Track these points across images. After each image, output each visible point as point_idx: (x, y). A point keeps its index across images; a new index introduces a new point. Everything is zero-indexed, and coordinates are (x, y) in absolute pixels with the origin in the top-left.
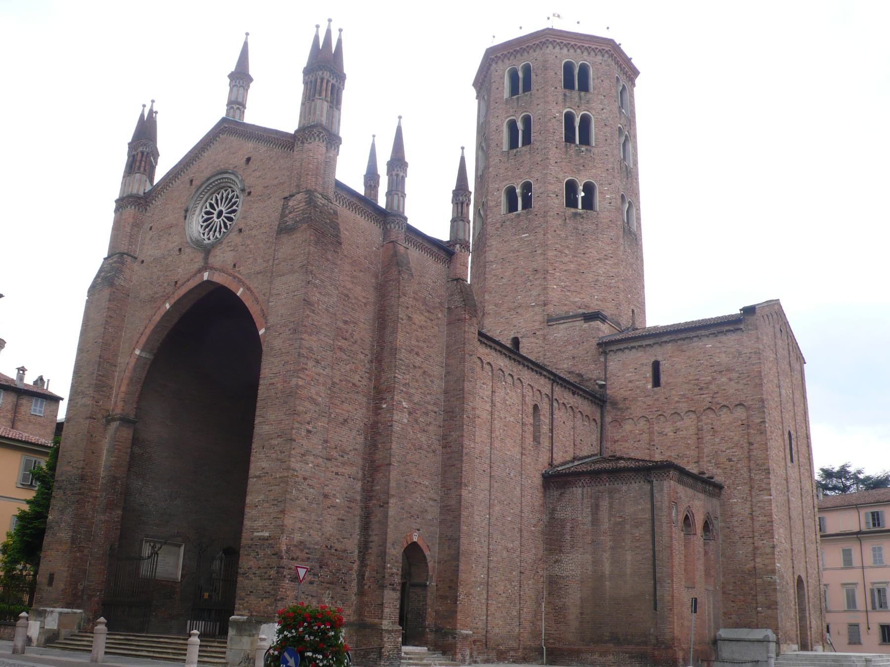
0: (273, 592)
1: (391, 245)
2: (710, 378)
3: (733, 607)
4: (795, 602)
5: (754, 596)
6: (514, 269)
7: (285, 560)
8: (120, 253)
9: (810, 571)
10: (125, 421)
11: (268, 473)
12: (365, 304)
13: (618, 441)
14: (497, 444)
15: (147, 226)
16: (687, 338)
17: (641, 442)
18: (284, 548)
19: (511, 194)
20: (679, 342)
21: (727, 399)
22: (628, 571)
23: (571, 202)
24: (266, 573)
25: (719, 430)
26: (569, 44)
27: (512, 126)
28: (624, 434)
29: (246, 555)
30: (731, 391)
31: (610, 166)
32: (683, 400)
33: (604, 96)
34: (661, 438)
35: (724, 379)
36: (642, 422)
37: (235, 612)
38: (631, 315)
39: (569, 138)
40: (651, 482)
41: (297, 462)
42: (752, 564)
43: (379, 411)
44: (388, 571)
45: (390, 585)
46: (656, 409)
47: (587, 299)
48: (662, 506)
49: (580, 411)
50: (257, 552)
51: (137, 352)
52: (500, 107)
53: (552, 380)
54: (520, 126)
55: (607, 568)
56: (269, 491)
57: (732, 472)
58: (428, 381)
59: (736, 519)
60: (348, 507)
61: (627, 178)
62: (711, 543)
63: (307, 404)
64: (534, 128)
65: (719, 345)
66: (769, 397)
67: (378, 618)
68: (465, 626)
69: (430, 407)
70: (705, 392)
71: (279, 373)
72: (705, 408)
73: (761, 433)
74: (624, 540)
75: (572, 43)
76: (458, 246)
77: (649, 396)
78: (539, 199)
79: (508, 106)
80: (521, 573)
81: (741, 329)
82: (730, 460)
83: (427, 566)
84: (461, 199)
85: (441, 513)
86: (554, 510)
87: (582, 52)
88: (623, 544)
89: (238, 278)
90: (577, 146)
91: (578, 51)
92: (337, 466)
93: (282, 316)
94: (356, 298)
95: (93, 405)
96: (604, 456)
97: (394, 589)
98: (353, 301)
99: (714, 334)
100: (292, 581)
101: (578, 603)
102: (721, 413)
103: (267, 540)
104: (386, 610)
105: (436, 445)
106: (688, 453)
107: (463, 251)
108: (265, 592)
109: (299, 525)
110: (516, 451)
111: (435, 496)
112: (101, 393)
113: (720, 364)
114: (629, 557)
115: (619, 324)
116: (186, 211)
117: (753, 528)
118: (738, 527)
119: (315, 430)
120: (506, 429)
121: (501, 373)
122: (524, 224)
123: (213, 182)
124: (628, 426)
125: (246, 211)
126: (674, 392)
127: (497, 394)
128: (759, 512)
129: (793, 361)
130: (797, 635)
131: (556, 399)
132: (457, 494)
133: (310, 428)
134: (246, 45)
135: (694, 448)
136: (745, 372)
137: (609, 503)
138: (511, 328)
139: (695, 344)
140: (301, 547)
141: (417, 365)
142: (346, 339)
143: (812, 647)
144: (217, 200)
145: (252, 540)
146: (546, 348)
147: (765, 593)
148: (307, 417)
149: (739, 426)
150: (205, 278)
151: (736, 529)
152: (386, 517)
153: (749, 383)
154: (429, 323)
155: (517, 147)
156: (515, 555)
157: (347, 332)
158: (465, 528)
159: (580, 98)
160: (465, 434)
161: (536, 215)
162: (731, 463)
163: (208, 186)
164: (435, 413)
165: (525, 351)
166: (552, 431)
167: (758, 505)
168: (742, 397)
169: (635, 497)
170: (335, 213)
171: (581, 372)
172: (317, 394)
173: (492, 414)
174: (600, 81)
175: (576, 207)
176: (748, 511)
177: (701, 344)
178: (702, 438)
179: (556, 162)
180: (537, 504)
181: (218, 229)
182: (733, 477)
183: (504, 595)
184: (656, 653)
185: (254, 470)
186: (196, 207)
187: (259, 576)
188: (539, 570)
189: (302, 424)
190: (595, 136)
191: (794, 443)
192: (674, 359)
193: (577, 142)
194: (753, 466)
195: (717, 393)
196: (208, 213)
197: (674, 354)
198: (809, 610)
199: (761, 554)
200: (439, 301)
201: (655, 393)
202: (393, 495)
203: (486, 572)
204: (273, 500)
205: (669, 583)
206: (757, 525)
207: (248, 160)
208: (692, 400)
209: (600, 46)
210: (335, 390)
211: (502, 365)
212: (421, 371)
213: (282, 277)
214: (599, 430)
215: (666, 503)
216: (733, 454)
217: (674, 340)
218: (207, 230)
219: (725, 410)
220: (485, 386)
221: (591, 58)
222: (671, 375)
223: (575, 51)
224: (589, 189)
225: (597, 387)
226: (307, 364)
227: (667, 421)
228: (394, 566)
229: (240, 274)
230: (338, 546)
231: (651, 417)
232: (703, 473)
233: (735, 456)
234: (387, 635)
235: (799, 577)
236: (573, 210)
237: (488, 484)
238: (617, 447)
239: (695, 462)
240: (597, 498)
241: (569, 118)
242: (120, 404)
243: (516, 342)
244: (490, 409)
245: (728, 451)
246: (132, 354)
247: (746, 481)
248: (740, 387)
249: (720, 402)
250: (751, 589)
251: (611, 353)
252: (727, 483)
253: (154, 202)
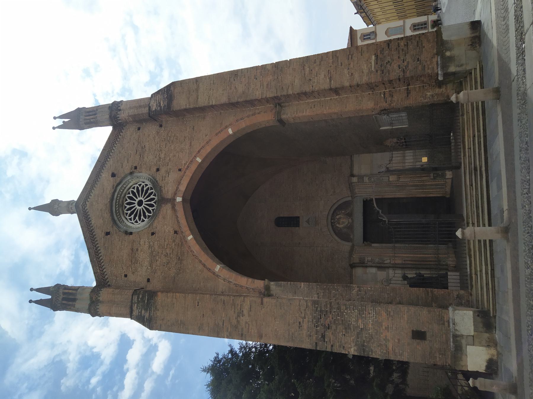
0: (417, 39)
11: (328, 71)
24: (403, 50)
29: (389, 74)
56: (341, 65)
71: (261, 81)
108: (418, 46)
186: (127, 225)
187: (405, 56)
213: (199, 97)
246: (217, 276)
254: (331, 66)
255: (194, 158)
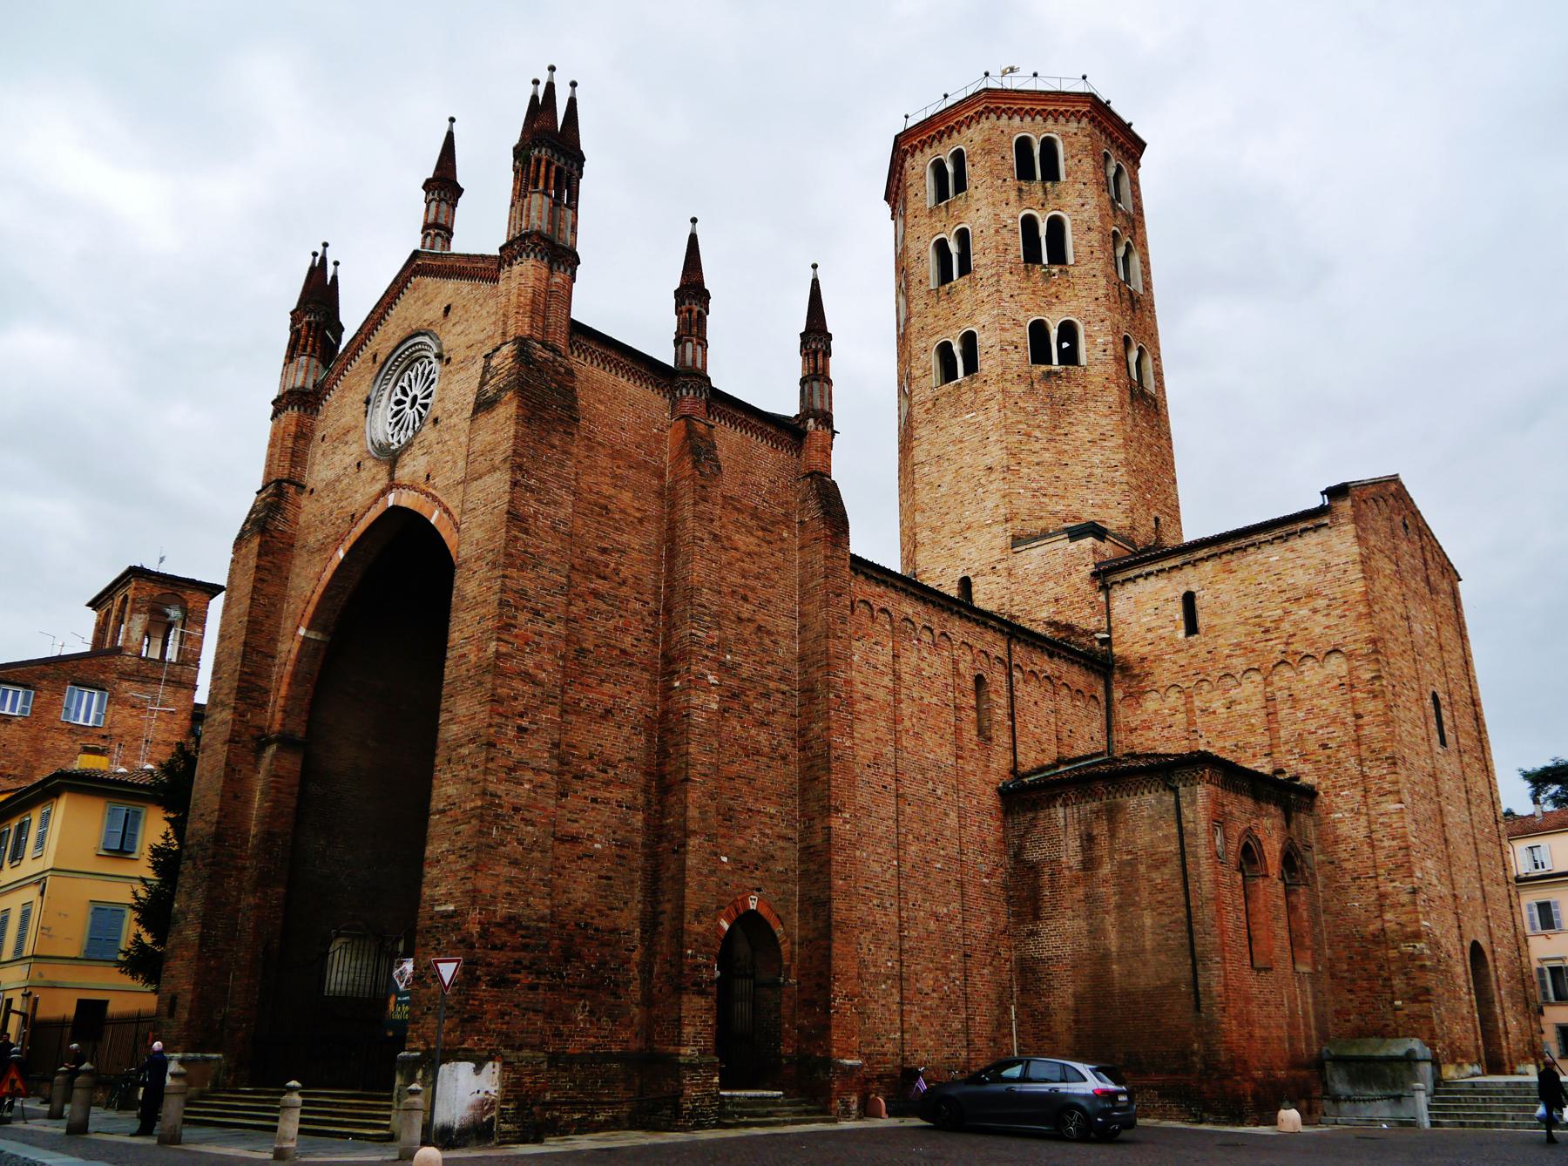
1: (682, 421)
2: (1280, 612)
3: (1351, 1000)
4: (1469, 989)
5: (1385, 979)
6: (957, 471)
7: (477, 950)
8: (276, 481)
9: (1498, 933)
10: (286, 742)
12: (641, 521)
13: (1136, 729)
14: (907, 742)
15: (319, 435)
16: (1236, 549)
17: (1173, 728)
18: (476, 929)
19: (945, 350)
20: (1225, 558)
21: (1312, 644)
22: (1148, 944)
23: (1040, 351)
25: (1302, 697)
26: (1021, 109)
27: (941, 246)
28: (1146, 717)
30: (1318, 630)
31: (1101, 292)
32: (1238, 652)
33: (1085, 184)
34: (1207, 719)
35: (1304, 612)
36: (1173, 694)
37: (407, 1046)
38: (1154, 526)
39: (1032, 255)
40: (1175, 790)
41: (500, 781)
42: (1378, 924)
43: (671, 693)
44: (689, 961)
45: (693, 985)
46: (1194, 672)
47: (1076, 506)
48: (1196, 830)
49: (1064, 684)
50: (438, 939)
51: (302, 631)
52: (922, 222)
53: (1007, 633)
54: (953, 247)
55: (1113, 941)
56: (457, 834)
57: (1331, 766)
58: (767, 641)
59: (1343, 847)
60: (618, 856)
61: (1134, 311)
62: (1301, 890)
63: (517, 684)
64: (975, 247)
65: (1292, 555)
66: (1388, 636)
67: (674, 1045)
68: (848, 1053)
69: (772, 685)
70: (1273, 636)
72: (1275, 662)
73: (1375, 697)
74: (1137, 890)
75: (1027, 107)
76: (811, 421)
77: (1182, 650)
78: (988, 356)
79: (934, 220)
80: (966, 955)
81: (1327, 524)
82: (1325, 747)
83: (779, 951)
84: (813, 347)
85: (801, 861)
86: (1021, 848)
87: (1045, 120)
88: (1137, 898)
89: (433, 495)
90: (1044, 267)
91: (1039, 118)
92: (594, 788)
93: (477, 544)
94: (622, 511)
95: (234, 721)
96: (1115, 755)
97: (701, 993)
98: (617, 517)
99: (1281, 537)
100: (492, 986)
101: (1070, 1003)
102: (1303, 668)
103: (452, 917)
104: (688, 1030)
105: (787, 746)
106: (1253, 740)
107: (820, 427)
109: (507, 889)
110: (945, 754)
111: (789, 833)
112: (249, 701)
113: (1294, 587)
114: (1148, 921)
115: (1132, 543)
116: (367, 402)
117: (1375, 861)
118: (1349, 860)
119: (534, 727)
120: (923, 716)
121: (909, 625)
122: (968, 397)
123: (403, 353)
124: (1151, 703)
125: (443, 390)
126: (1221, 641)
127: (902, 660)
128: (1383, 833)
129: (1434, 577)
130: (1477, 1047)
131: (1018, 666)
132: (824, 825)
133: (525, 724)
134: (450, 137)
135: (1262, 730)
136: (1339, 595)
137: (1109, 830)
138: (958, 563)
139: (1251, 558)
140: (512, 927)
141: (745, 615)
142: (604, 578)
143: (1512, 1068)
144: (410, 380)
145: (431, 918)
146: (1012, 590)
147: (1405, 974)
148: (519, 706)
149: (1335, 688)
150: (390, 504)
151: (1347, 865)
152: (682, 868)
153: (1347, 613)
154: (765, 548)
155: (952, 280)
156: (952, 927)
157: (607, 566)
158: (841, 882)
159: (1045, 192)
160: (834, 725)
161: (985, 381)
162: (1328, 752)
163: (396, 360)
164: (784, 693)
165: (981, 596)
166: (1012, 717)
167: (1381, 820)
168: (1336, 638)
169: (1150, 817)
170: (570, 373)
171: (1069, 622)
172: (539, 666)
173: (895, 692)
174: (1077, 161)
175: (1050, 362)
176: (1363, 832)
177: (1260, 556)
178: (1275, 713)
179: (1012, 296)
180: (990, 839)
181: (411, 426)
182: (1332, 776)
183: (935, 995)
184: (1205, 1087)
185: (437, 803)
188: (1002, 950)
189: (507, 717)
190: (1074, 248)
191: (1445, 713)
192: (1218, 587)
193: (1045, 260)
194: (1365, 754)
195: (1294, 635)
196: (399, 402)
197: (1217, 578)
198: (1501, 1001)
199: (1393, 906)
200: (783, 511)
201: (1191, 646)
202: (694, 833)
203: (896, 957)
204: (461, 849)
205: (1217, 963)
206: (1381, 856)
207: (448, 309)
208: (1253, 651)
209: (1074, 107)
210: (586, 661)
211: (910, 611)
212: (752, 627)
213: (479, 482)
214: (1104, 714)
215: (1203, 825)
216: (1330, 735)
217: (1215, 555)
218: (397, 428)
219: (1310, 662)
220: (880, 648)
221: (1060, 127)
222: (1215, 614)
223: (1033, 119)
224: (1068, 331)
225: (1097, 644)
226: (515, 617)
227: (1214, 689)
228: (701, 952)
229: (435, 489)
230: (600, 922)
231: (1186, 685)
232: (1281, 772)
233: (1334, 738)
234: (689, 1074)
235: (1476, 946)
236: (1044, 368)
237: (893, 808)
238: (1135, 739)
239: (1265, 755)
240: (1089, 825)
241: (1029, 224)
242: (279, 716)
243: (965, 584)
244: (891, 685)
245: (1320, 732)
247: (1355, 781)
248: (1332, 621)
249: (1300, 649)
250: (1381, 967)
251: (1115, 586)
252: (1323, 785)
253: (328, 397)
254: (460, 807)
255: (439, 501)
